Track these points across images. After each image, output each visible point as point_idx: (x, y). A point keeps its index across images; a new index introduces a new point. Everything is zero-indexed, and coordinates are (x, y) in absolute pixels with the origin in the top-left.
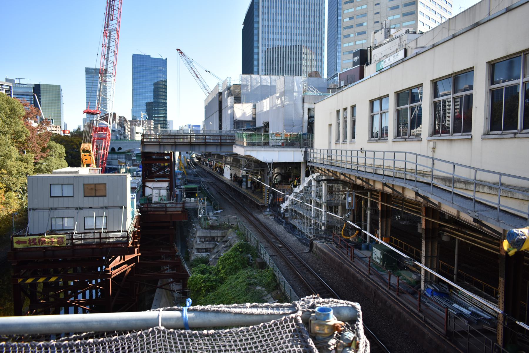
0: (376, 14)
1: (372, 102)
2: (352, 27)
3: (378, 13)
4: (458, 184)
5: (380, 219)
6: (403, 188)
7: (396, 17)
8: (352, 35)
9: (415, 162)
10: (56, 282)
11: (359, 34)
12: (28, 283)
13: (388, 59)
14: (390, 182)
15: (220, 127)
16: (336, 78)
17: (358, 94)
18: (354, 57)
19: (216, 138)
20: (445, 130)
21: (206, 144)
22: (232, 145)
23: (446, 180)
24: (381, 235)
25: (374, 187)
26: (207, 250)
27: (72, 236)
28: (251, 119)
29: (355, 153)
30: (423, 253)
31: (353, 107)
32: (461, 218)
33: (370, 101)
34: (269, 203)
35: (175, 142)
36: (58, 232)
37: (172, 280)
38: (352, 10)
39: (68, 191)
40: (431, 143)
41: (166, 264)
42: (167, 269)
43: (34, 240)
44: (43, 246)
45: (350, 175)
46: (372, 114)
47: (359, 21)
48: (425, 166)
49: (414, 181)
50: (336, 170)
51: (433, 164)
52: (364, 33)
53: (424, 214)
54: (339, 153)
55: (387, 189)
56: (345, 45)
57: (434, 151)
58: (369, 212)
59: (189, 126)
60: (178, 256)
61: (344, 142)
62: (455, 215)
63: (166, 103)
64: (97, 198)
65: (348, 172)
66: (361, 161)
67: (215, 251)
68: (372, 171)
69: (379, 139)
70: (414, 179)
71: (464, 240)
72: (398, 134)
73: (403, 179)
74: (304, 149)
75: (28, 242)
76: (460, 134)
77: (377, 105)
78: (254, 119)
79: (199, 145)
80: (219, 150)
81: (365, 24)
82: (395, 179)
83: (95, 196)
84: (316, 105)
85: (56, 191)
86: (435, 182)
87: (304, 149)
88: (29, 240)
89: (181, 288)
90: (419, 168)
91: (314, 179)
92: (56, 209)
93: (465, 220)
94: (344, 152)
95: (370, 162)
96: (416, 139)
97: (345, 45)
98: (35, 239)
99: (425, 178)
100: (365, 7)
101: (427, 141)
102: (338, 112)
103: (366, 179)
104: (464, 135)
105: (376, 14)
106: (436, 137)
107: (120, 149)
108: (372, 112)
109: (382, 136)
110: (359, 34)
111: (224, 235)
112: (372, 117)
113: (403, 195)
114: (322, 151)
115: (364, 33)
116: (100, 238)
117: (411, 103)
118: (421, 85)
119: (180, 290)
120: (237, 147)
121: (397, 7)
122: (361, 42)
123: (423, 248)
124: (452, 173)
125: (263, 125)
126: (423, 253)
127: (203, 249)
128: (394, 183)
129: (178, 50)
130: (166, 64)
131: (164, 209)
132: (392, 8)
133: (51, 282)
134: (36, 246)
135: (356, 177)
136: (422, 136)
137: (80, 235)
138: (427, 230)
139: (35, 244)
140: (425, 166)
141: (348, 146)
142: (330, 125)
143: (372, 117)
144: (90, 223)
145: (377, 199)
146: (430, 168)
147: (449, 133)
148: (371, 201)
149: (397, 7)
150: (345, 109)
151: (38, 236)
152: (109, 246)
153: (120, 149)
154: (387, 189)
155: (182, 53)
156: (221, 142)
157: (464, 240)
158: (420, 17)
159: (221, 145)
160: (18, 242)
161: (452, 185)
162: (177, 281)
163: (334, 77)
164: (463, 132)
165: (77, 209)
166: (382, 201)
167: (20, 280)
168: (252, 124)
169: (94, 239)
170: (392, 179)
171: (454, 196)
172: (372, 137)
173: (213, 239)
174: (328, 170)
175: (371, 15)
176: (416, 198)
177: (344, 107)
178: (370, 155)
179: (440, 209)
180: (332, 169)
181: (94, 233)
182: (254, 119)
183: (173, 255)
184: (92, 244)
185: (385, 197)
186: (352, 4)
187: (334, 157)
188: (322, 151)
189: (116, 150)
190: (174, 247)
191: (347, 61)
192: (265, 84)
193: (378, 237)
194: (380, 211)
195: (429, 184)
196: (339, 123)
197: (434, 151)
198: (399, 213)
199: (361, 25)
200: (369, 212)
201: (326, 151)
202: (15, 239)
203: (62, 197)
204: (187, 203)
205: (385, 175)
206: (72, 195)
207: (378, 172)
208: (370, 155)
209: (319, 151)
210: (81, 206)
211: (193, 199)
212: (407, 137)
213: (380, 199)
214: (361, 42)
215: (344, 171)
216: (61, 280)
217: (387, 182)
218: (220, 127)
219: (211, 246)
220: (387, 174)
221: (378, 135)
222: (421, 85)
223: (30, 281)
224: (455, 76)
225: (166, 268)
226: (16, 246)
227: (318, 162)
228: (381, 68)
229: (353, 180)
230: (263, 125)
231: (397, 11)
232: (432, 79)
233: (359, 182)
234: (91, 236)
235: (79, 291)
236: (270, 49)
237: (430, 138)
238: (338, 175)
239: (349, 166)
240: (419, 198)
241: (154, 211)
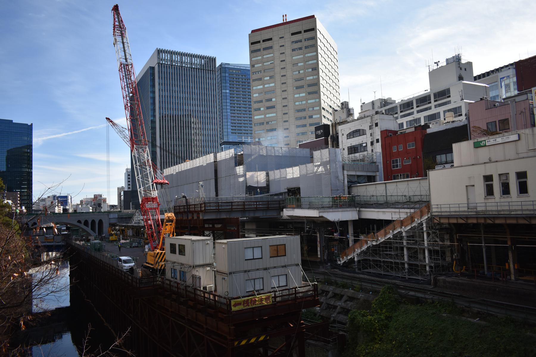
0: (283, 91)
2: (261, 101)
3: (286, 91)
7: (301, 95)
8: (262, 109)
10: (265, 340)
11: (268, 108)
12: (261, 341)
15: (217, 195)
16: (223, 146)
19: (264, 203)
28: (265, 185)
34: (325, 258)
35: (256, 208)
38: (261, 87)
39: (257, 253)
43: (248, 300)
44: (254, 306)
47: (268, 96)
52: (273, 107)
56: (256, 117)
63: (32, 172)
64: (279, 258)
74: (358, 209)
78: (268, 185)
79: (249, 211)
80: (264, 215)
81: (274, 100)
85: (249, 254)
87: (358, 209)
91: (406, 232)
92: (249, 271)
97: (256, 117)
100: (273, 85)
105: (283, 91)
110: (268, 108)
115: (273, 107)
121: (302, 87)
122: (271, 115)
125: (286, 191)
129: (107, 118)
130: (32, 130)
132: (297, 88)
134: (247, 307)
149: (302, 87)
155: (112, 122)
156: (232, 209)
158: (322, 97)
159: (268, 209)
165: (266, 269)
167: (236, 343)
168: (266, 190)
175: (278, 91)
177: (488, 174)
182: (268, 185)
184: (288, 300)
186: (260, 82)
191: (258, 132)
192: (277, 154)
199: (270, 100)
203: (254, 259)
210: (268, 266)
214: (271, 115)
216: (268, 338)
218: (217, 195)
223: (244, 342)
226: (234, 309)
230: (286, 191)
231: (302, 90)
234: (286, 292)
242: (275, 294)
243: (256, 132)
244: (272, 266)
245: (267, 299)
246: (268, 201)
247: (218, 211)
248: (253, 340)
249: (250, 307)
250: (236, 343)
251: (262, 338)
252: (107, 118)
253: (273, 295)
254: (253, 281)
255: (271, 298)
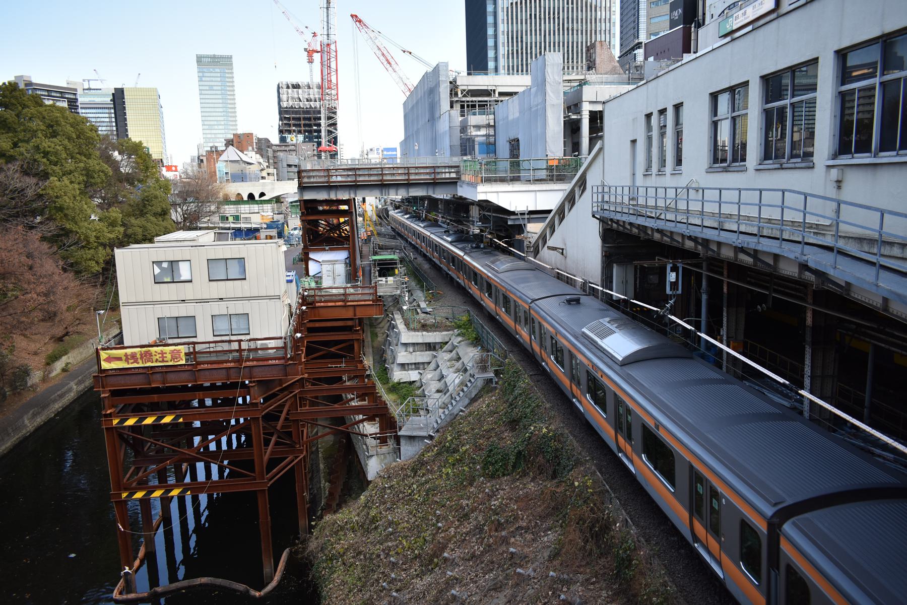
1: (714, 96)
4: (888, 248)
5: (725, 309)
6: (776, 257)
9: (802, 209)
10: (172, 424)
12: (130, 427)
13: (743, 11)
14: (751, 243)
16: (636, 52)
17: (689, 83)
18: (671, 11)
20: (864, 147)
21: (408, 185)
22: (453, 183)
23: (860, 240)
24: (728, 337)
25: (719, 254)
26: (417, 366)
27: (194, 348)
29: (683, 194)
30: (807, 370)
31: (678, 107)
32: (891, 310)
33: (711, 94)
36: (170, 341)
37: (361, 417)
40: (834, 173)
41: (350, 389)
42: (353, 399)
43: (133, 356)
45: (672, 233)
46: (716, 119)
48: (817, 215)
49: (799, 242)
50: (647, 224)
51: (838, 211)
53: (810, 300)
54: (651, 192)
55: (743, 257)
57: (839, 187)
58: (704, 297)
59: (378, 149)
60: (369, 376)
61: (661, 173)
62: (879, 305)
65: (669, 227)
66: (695, 207)
67: (433, 365)
68: (716, 225)
69: (729, 166)
70: (800, 239)
71: (887, 347)
72: (767, 156)
73: (778, 239)
75: (124, 358)
76: (894, 153)
77: (724, 101)
79: (397, 186)
82: (761, 239)
83: (228, 280)
84: (607, 105)
86: (841, 244)
88: (126, 355)
89: (378, 431)
90: (810, 219)
93: (899, 314)
94: (661, 192)
95: (711, 208)
96: (803, 165)
98: (135, 353)
99: (821, 238)
101: (824, 169)
102: (649, 116)
103: (703, 239)
104: (902, 155)
106: (845, 160)
107: (262, 194)
108: (716, 115)
109: (734, 160)
111: (447, 340)
112: (715, 125)
113: (775, 267)
114: (619, 190)
116: (240, 350)
117: (793, 96)
118: (815, 61)
119: (376, 434)
120: (465, 186)
123: (808, 362)
124: (878, 228)
126: (807, 370)
127: (411, 364)
128: (759, 248)
129: (352, 16)
131: (342, 297)
133: (165, 424)
134: (136, 365)
135: (683, 236)
136: (815, 159)
137: (207, 345)
138: (814, 327)
139: (136, 361)
140: (817, 215)
141: (668, 181)
142: (634, 142)
143: (715, 125)
144: (223, 326)
145: (722, 274)
146: (828, 218)
147: (869, 151)
148: (709, 277)
150: (662, 112)
151: (139, 349)
152: (255, 363)
153: (262, 194)
154: (743, 257)
155: (360, 21)
157: (887, 347)
160: (109, 359)
161: (875, 251)
162: (371, 419)
163: (633, 49)
164: (901, 149)
166: (728, 277)
169: (231, 351)
170: (755, 239)
171: (881, 271)
172: (715, 160)
173: (430, 347)
174: (631, 224)
176: (800, 273)
178: (712, 195)
179: (848, 295)
180: (640, 221)
181: (230, 341)
183: (361, 375)
185: (736, 269)
187: (641, 201)
188: (619, 190)
189: (257, 198)
190: (361, 362)
191: (656, 20)
193: (721, 342)
194: (725, 296)
195: (829, 249)
196: (650, 139)
197: (839, 187)
198: (762, 298)
200: (704, 297)
201: (626, 190)
202: (103, 355)
204: (381, 285)
205: (741, 233)
206: (189, 278)
207: (727, 227)
208: (712, 195)
209: (613, 190)
211: (391, 279)
212: (785, 160)
213: (725, 273)
215: (660, 225)
216: (181, 420)
217: (745, 245)
219: (426, 360)
220: (743, 230)
221: (727, 157)
222: (815, 61)
223: (131, 422)
224: (885, 41)
225: (350, 396)
226: (105, 365)
227: (612, 209)
228: (729, 29)
229: (678, 242)
232: (836, 48)
233: (689, 244)
234: (226, 347)
235: (210, 437)
236: (516, 3)
237: (831, 163)
238: (650, 232)
239: (670, 216)
240: (807, 273)
241: (325, 301)
242: (194, 348)
243: (653, 21)
244: (216, 296)
245: (175, 355)
246: (328, 170)
247: (330, 187)
248: (149, 421)
249: (141, 365)
250: (115, 422)
251: (168, 419)
252: (352, 16)
253: (192, 350)
254: (174, 321)
255: (183, 355)
